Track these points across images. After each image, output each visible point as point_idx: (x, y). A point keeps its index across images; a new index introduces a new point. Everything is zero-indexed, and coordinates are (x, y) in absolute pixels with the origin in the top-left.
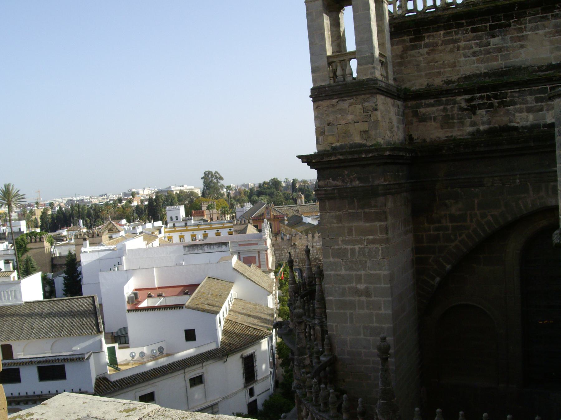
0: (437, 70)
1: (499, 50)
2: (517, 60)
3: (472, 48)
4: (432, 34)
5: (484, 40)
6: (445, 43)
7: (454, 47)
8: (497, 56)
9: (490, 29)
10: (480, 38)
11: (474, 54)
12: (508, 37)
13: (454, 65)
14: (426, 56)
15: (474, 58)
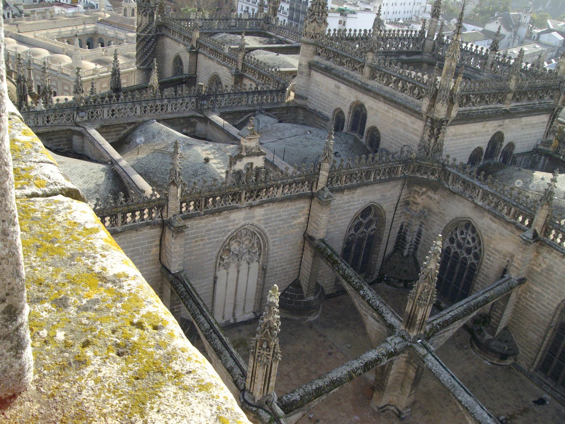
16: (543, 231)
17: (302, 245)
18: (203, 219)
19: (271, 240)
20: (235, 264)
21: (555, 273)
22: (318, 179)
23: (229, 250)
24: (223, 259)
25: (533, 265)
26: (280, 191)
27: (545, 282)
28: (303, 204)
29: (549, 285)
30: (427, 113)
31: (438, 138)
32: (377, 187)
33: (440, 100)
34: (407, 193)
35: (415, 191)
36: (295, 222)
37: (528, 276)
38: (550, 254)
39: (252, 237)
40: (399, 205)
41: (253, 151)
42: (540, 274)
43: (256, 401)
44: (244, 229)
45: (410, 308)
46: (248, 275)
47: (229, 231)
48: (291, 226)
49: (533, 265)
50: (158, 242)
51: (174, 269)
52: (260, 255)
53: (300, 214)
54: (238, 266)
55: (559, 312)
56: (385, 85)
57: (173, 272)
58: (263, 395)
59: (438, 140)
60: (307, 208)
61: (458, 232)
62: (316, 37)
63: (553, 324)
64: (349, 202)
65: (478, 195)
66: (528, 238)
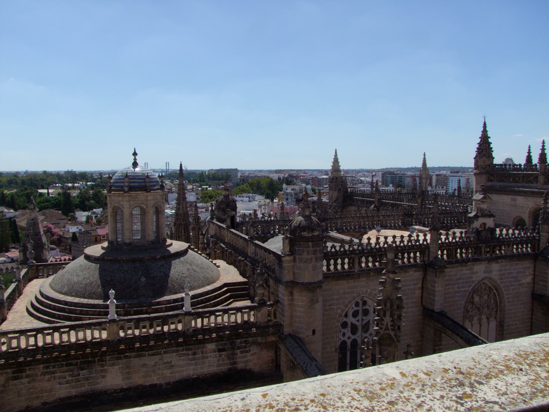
0: (36, 395)
1: (87, 379)
2: (100, 386)
3: (65, 378)
4: (33, 367)
5: (76, 372)
6: (44, 374)
7: (51, 377)
8: (85, 383)
9: (80, 364)
10: (72, 371)
11: (67, 382)
12: (94, 370)
13: (51, 390)
14: (27, 384)
15: (67, 385)
18: (454, 268)
19: (506, 297)
20: (477, 318)
23: (473, 303)
24: (468, 311)
26: (511, 248)
28: (528, 264)
36: (524, 281)
39: (490, 293)
41: (486, 213)
44: (484, 283)
46: (488, 330)
47: (473, 282)
48: (520, 285)
50: (420, 285)
51: (437, 307)
52: (496, 311)
54: (480, 320)
57: (435, 310)
60: (532, 269)
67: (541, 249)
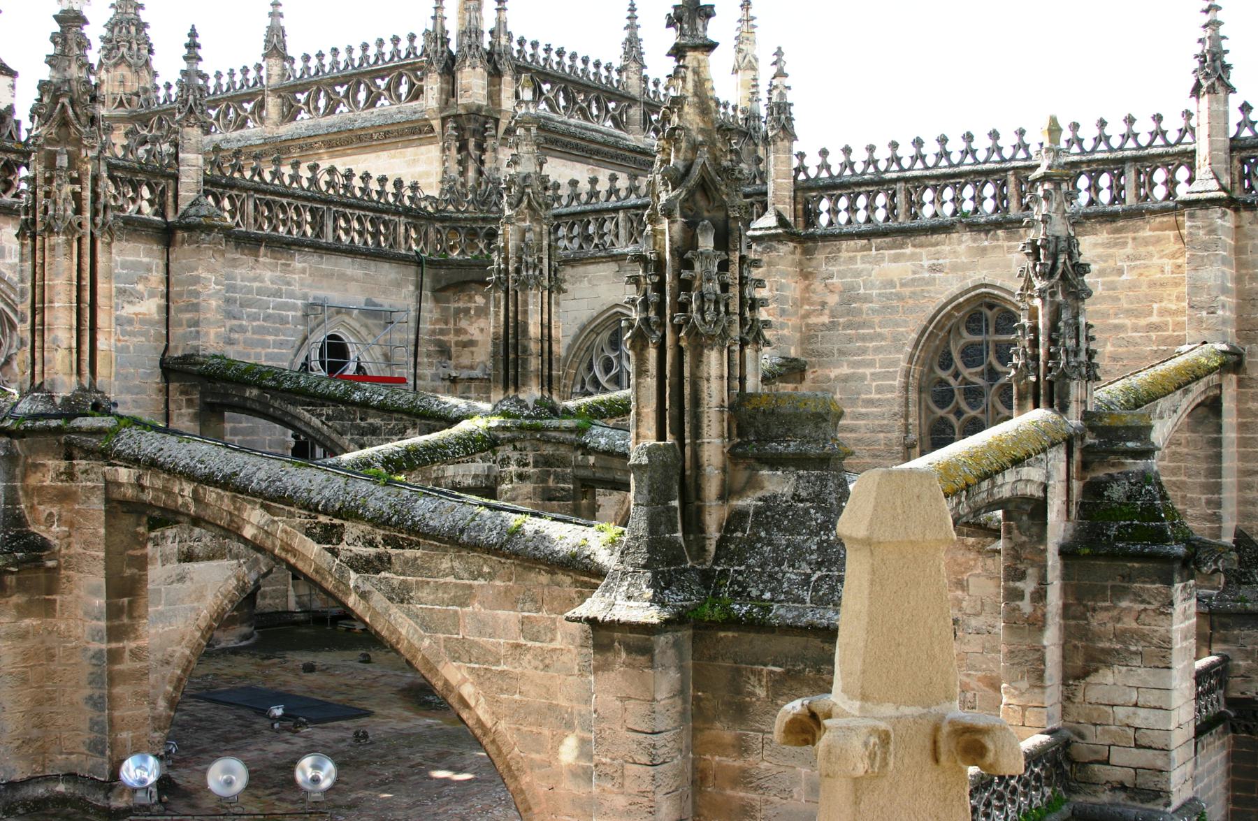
16: (800, 213)
17: (161, 398)
21: (867, 299)
22: (176, 178)
25: (807, 315)
27: (850, 340)
29: (863, 338)
30: (441, 110)
31: (482, 162)
32: (348, 267)
33: (464, 61)
34: (436, 315)
35: (458, 311)
37: (804, 352)
38: (835, 259)
40: (422, 349)
42: (833, 326)
43: (58, 401)
45: (502, 318)
49: (807, 315)
53: (140, 287)
55: (913, 396)
56: (325, 114)
58: (79, 383)
59: (486, 169)
60: (157, 276)
61: (597, 370)
62: (129, 102)
63: (913, 436)
64: (278, 294)
65: (617, 236)
66: (770, 228)
67: (183, 206)
